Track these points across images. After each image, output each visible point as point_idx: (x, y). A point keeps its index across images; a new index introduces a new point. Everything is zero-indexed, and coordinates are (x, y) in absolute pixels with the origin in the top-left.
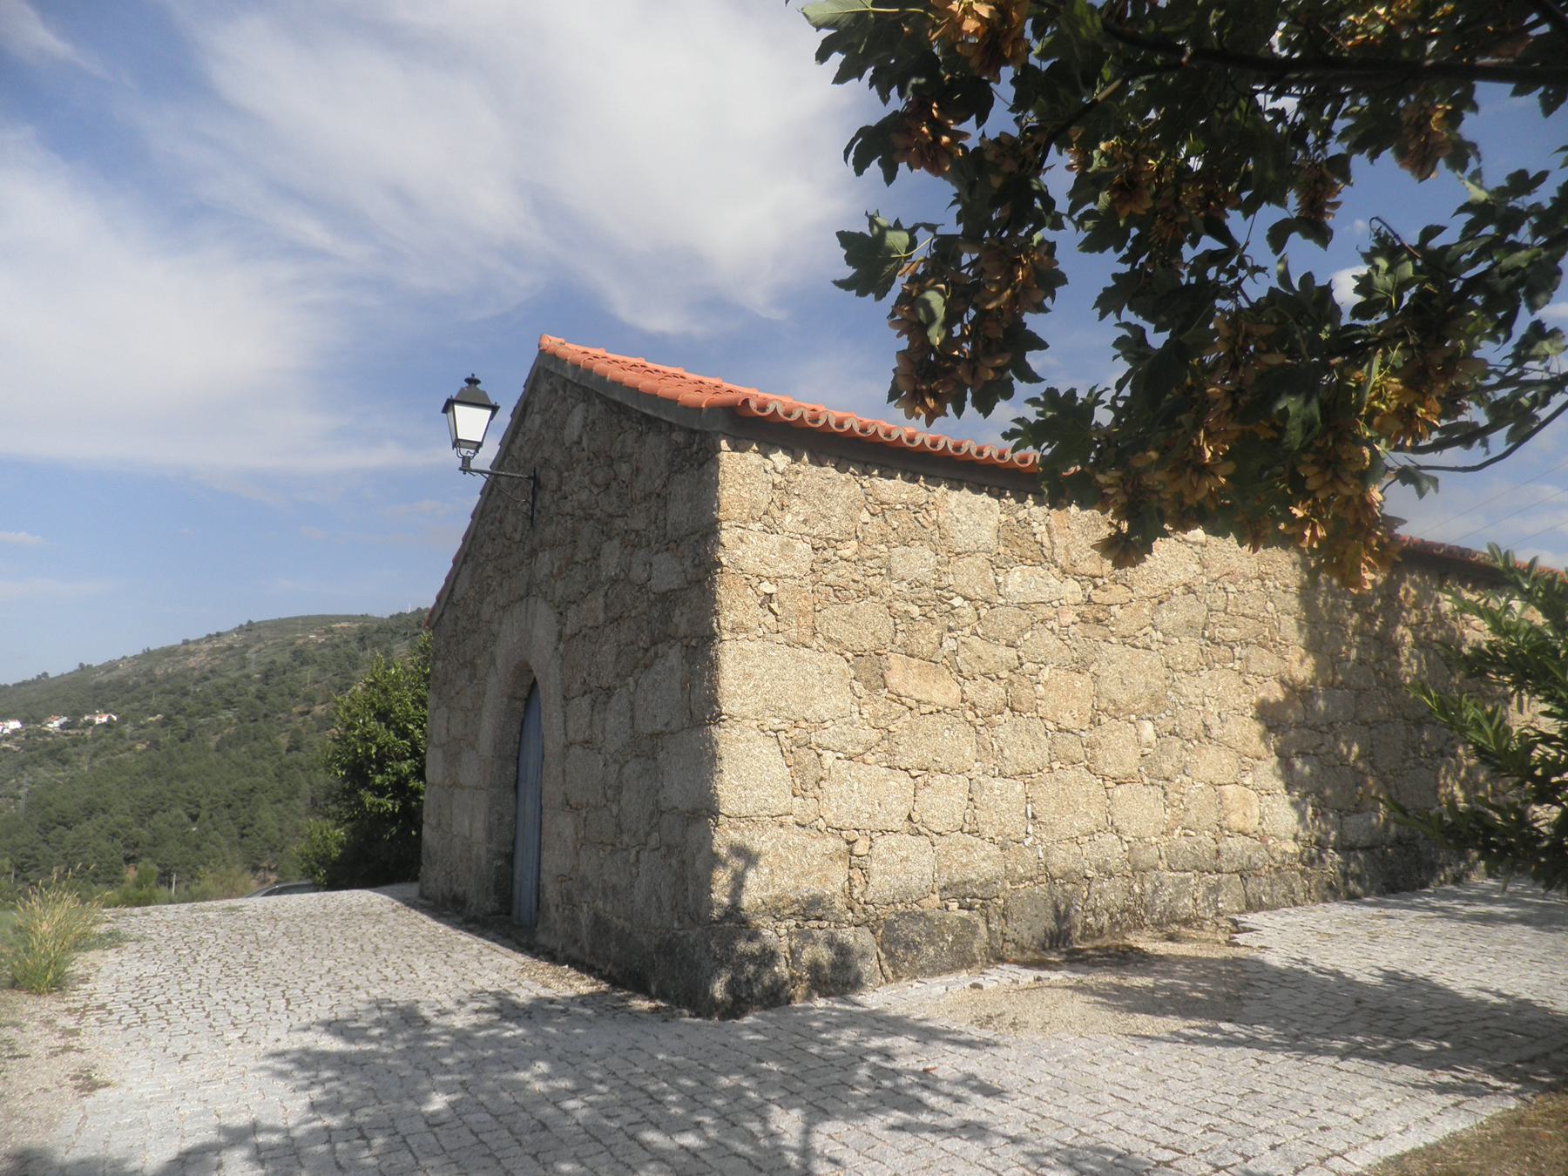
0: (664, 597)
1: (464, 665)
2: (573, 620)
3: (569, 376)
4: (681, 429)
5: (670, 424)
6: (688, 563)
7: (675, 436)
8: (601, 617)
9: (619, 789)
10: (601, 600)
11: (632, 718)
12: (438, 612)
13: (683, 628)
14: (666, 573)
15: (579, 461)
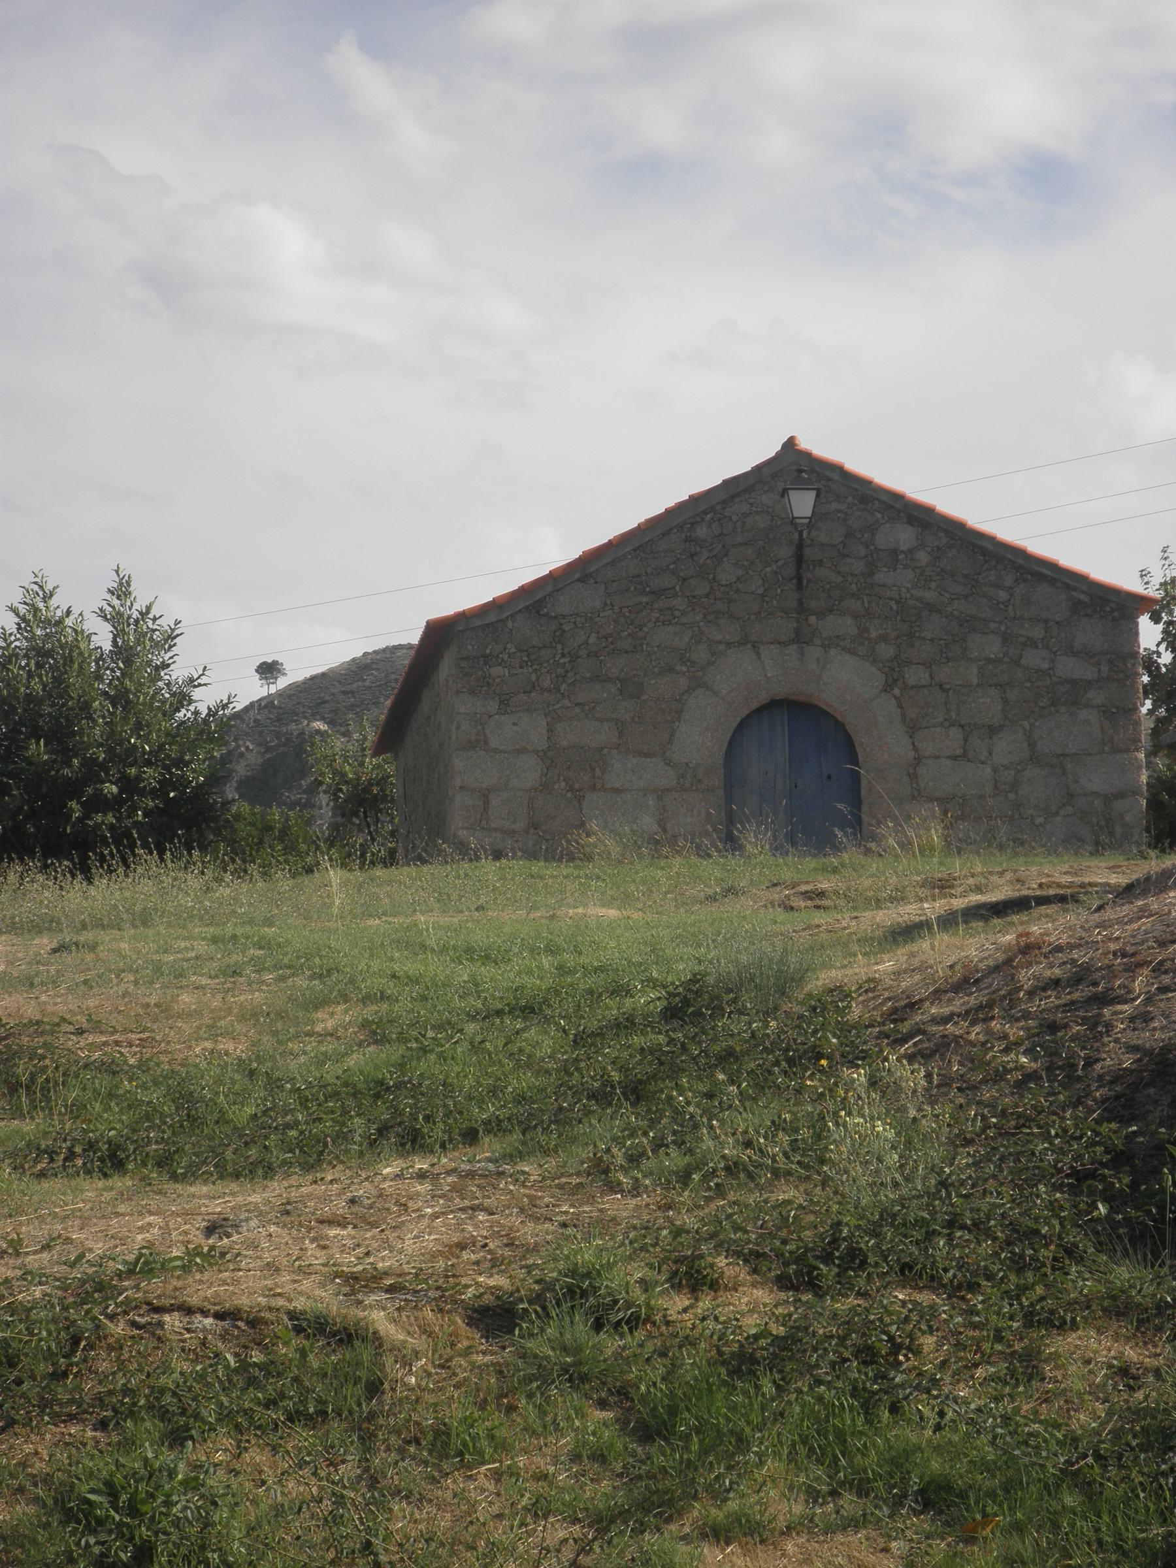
0: (1074, 682)
1: (595, 678)
2: (915, 675)
3: (884, 498)
4: (1083, 592)
5: (1068, 586)
6: (1105, 669)
7: (1075, 594)
8: (975, 681)
9: (1015, 785)
10: (974, 669)
11: (1032, 745)
12: (491, 618)
13: (1099, 700)
14: (1068, 667)
15: (906, 567)
